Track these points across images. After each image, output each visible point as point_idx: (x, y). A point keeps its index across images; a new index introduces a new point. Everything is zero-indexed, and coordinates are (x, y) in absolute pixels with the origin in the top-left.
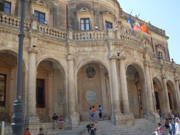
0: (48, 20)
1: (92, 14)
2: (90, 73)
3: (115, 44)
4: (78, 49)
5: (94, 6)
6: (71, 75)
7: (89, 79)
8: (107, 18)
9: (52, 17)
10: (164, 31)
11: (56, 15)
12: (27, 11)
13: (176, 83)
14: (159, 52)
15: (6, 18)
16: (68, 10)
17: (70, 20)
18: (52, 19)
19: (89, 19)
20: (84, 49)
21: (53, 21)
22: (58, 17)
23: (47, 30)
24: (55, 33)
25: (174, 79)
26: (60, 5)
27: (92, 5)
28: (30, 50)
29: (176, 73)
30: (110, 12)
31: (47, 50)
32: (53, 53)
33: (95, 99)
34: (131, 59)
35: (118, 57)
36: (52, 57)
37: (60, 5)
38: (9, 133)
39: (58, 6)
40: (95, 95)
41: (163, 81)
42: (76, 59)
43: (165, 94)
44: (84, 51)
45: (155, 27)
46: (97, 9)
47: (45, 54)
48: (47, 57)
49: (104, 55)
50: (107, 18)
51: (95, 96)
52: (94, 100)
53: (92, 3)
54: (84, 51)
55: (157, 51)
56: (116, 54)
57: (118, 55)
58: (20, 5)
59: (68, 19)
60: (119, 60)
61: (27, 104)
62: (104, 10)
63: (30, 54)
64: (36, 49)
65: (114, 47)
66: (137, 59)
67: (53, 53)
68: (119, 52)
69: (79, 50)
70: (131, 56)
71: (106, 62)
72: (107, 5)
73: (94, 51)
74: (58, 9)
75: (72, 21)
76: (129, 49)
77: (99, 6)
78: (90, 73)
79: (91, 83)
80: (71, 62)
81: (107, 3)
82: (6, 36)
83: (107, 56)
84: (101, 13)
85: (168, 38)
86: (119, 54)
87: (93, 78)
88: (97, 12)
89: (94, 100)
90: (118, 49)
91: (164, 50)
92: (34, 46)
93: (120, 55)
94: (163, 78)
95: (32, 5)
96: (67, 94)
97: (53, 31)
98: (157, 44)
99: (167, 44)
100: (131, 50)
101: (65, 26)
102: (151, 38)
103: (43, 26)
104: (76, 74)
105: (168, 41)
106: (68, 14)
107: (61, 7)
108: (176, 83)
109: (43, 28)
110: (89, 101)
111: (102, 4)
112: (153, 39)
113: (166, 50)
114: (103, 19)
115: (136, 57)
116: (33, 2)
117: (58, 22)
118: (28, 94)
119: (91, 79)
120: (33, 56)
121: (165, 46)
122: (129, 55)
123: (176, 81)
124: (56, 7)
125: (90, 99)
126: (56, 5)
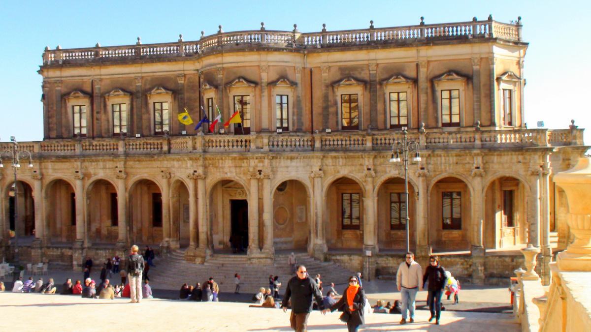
22: (185, 101)
26: (188, 79)
31: (138, 171)
32: (147, 173)
35: (192, 176)
36: (144, 178)
37: (188, 79)
46: (222, 80)
47: (137, 175)
48: (141, 178)
56: (192, 171)
57: (194, 174)
58: (135, 104)
62: (231, 79)
65: (191, 162)
66: (231, 172)
67: (147, 173)
68: (195, 170)
70: (218, 171)
72: (239, 65)
77: (225, 73)
82: (97, 164)
92: (120, 171)
100: (220, 161)
101: (197, 112)
107: (191, 82)
115: (226, 170)
122: (215, 169)
124: (183, 85)
126: (182, 82)
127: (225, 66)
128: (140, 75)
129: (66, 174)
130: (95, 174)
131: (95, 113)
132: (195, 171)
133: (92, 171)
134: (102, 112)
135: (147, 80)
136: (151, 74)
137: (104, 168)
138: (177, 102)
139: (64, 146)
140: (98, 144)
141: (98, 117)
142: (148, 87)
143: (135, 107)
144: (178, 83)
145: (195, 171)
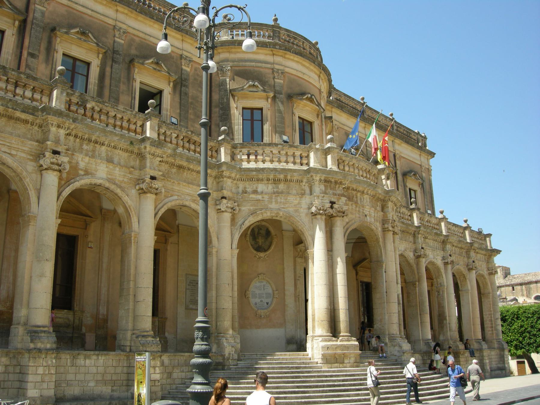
0: (169, 107)
1: (270, 100)
2: (260, 241)
3: (326, 181)
4: (241, 186)
5: (274, 78)
6: (226, 246)
7: (259, 253)
8: (304, 110)
9: (177, 99)
10: (425, 138)
11: (186, 94)
12: (124, 83)
13: (446, 269)
14: (410, 190)
15: (93, 109)
16: (213, 84)
17: (217, 109)
18: (178, 105)
19: (261, 109)
20: (257, 188)
21: (178, 111)
22: (190, 100)
23: (177, 137)
24: (192, 147)
25: (443, 258)
27: (271, 76)
28: (143, 186)
29: (447, 246)
30: (312, 95)
33: (269, 300)
34: (357, 215)
35: (330, 210)
38: (98, 373)
39: (191, 74)
40: (270, 291)
41: (418, 264)
42: (237, 208)
43: (421, 294)
44: (255, 192)
45: (404, 126)
47: (172, 196)
49: (299, 203)
50: (304, 110)
51: (269, 294)
52: (267, 303)
53: (271, 71)
54: (255, 192)
55: (405, 186)
57: (332, 207)
58: (108, 69)
59: (213, 104)
60: (331, 216)
61: (134, 310)
62: (297, 90)
63: (143, 196)
64: (157, 184)
68: (333, 200)
69: (245, 188)
70: (357, 209)
71: (302, 220)
73: (278, 193)
74: (191, 81)
75: (221, 112)
76: (354, 192)
78: (260, 241)
79: (263, 262)
80: (227, 216)
81: (304, 74)
83: (307, 206)
84: (290, 97)
85: (432, 154)
86: (332, 203)
87: (265, 251)
88: (281, 94)
89: (267, 303)
90: (331, 192)
91: (422, 185)
92: (153, 178)
93: (335, 206)
94: (418, 257)
95: (136, 70)
96: (214, 289)
97: (189, 142)
98: (406, 169)
99: (429, 170)
102: (394, 156)
103: (169, 129)
104: (235, 245)
105: (432, 161)
106: (213, 94)
107: (198, 75)
108: (446, 269)
109: (168, 133)
110: (256, 304)
111: (292, 74)
112: (397, 156)
113: (426, 185)
114: (293, 113)
116: (138, 62)
117: (190, 111)
118: (136, 287)
119: (262, 255)
120: (150, 199)
121: (424, 175)
122: (354, 206)
123: (446, 264)
125: (257, 300)
127: (287, 70)
128: (124, 26)
129: (14, 152)
130: (87, 173)
131: (25, 53)
132: (334, 203)
133: (82, 161)
134: (42, 57)
135: (133, 40)
136: (141, 35)
137: (110, 160)
138: (177, 96)
139: (16, 85)
140: (97, 109)
141: (29, 62)
142: (133, 52)
143: (108, 73)
144: (182, 69)
145: (334, 203)
